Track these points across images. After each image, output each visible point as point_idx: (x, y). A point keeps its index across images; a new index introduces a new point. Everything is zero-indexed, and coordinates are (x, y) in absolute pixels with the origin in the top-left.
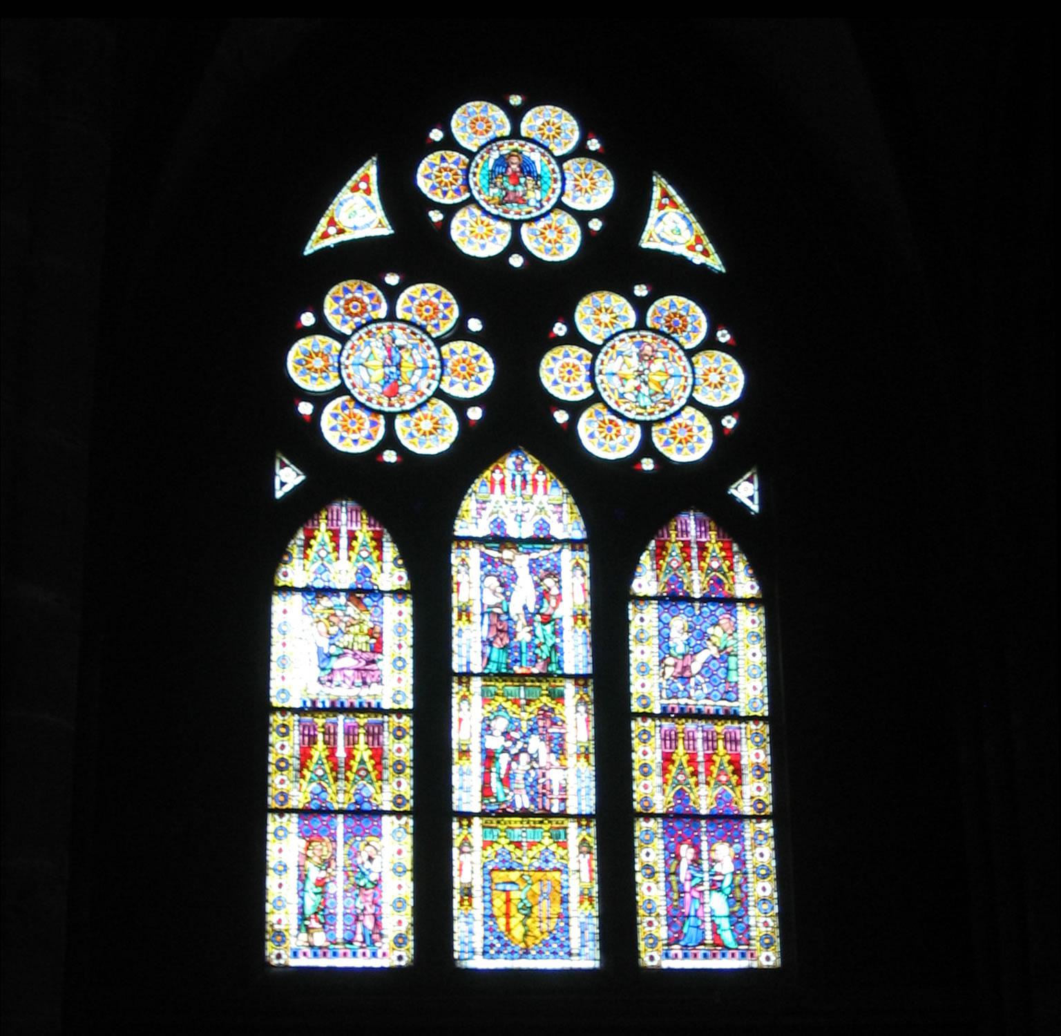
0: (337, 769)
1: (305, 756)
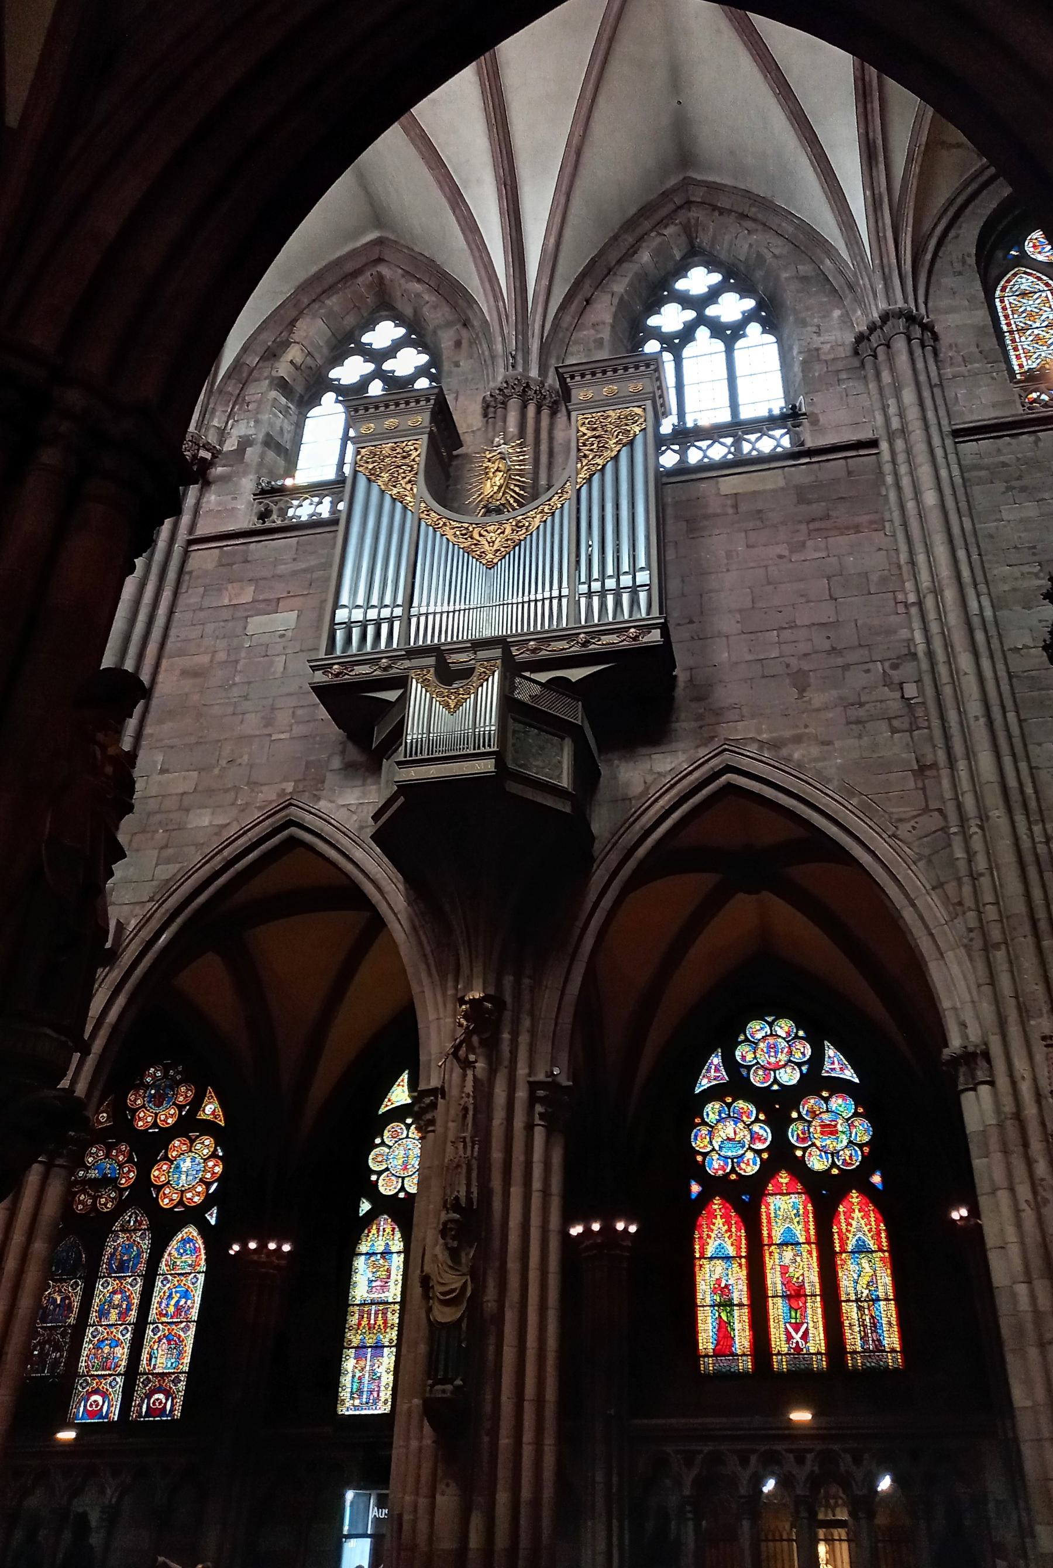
1: (359, 1324)
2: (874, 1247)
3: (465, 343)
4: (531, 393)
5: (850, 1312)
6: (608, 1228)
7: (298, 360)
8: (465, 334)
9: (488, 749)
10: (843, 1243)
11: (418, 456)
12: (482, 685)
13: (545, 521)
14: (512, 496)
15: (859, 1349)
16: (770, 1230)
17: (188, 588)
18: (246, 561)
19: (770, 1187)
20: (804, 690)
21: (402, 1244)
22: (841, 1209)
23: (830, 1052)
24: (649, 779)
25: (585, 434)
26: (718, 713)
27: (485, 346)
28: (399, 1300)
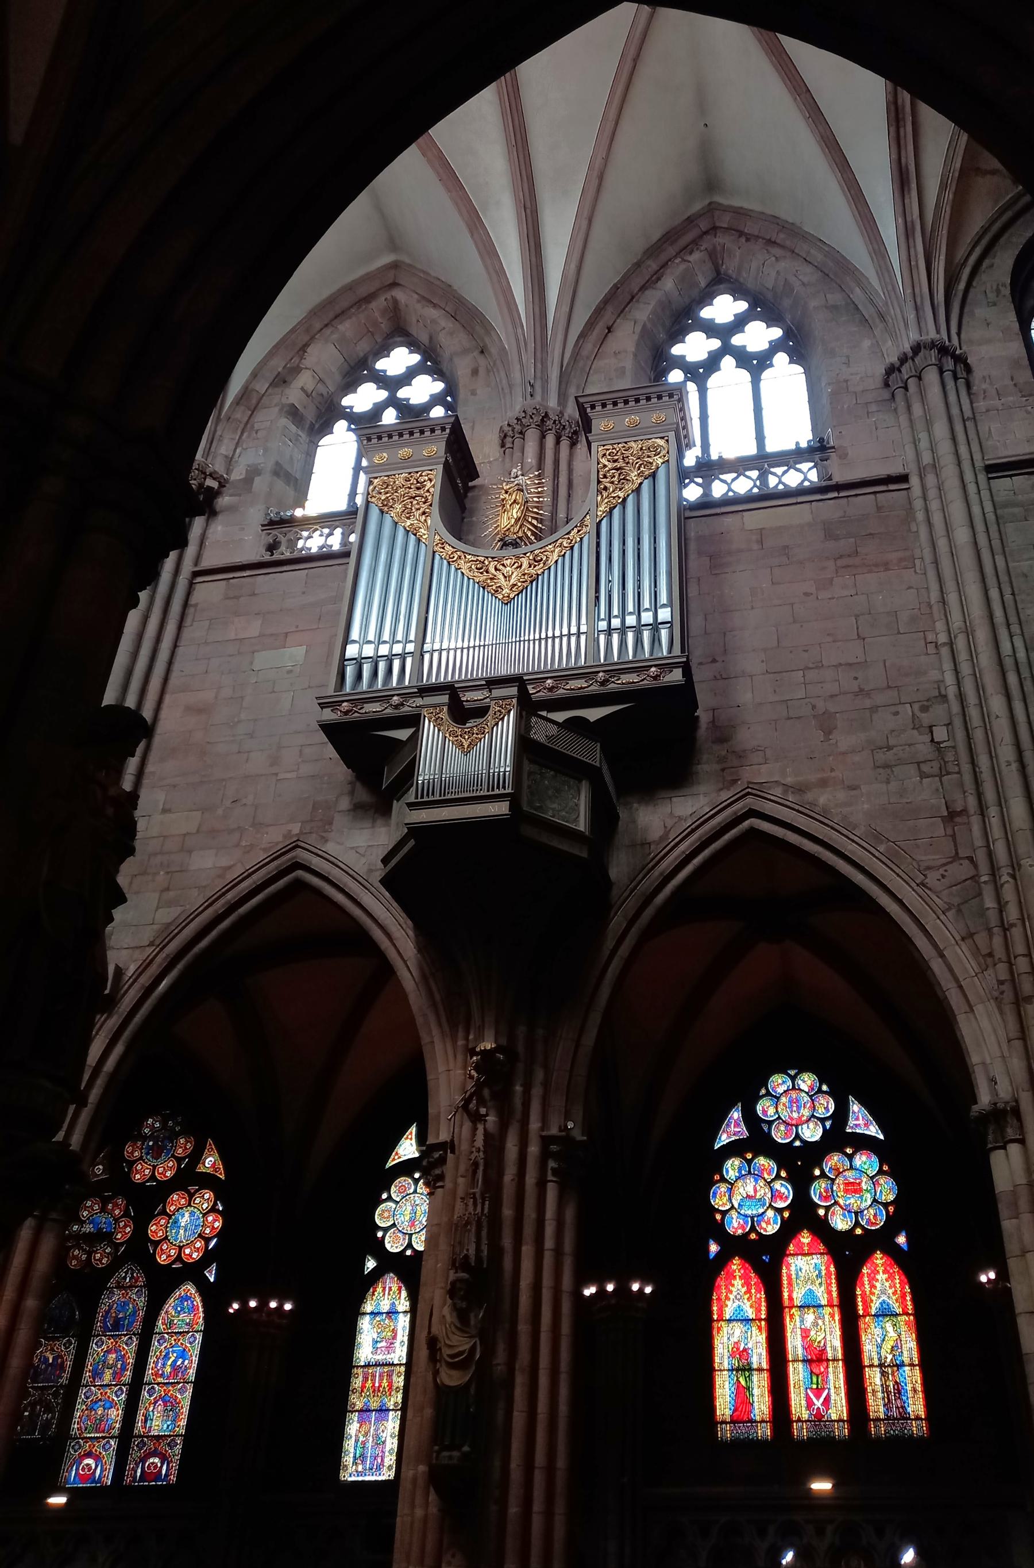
0: (375, 1390)
2: (899, 1311)
3: (482, 371)
4: (549, 423)
5: (874, 1378)
6: (623, 1289)
7: (310, 387)
8: (482, 361)
9: (502, 791)
10: (867, 1306)
11: (433, 486)
12: (497, 724)
13: (564, 556)
14: (529, 529)
15: (882, 1416)
16: (791, 1292)
17: (193, 621)
18: (254, 594)
19: (791, 1247)
20: (830, 733)
21: (408, 1303)
22: (865, 1270)
23: (855, 1107)
24: (669, 823)
25: (605, 466)
26: (741, 755)
27: (503, 374)
28: (404, 1361)
